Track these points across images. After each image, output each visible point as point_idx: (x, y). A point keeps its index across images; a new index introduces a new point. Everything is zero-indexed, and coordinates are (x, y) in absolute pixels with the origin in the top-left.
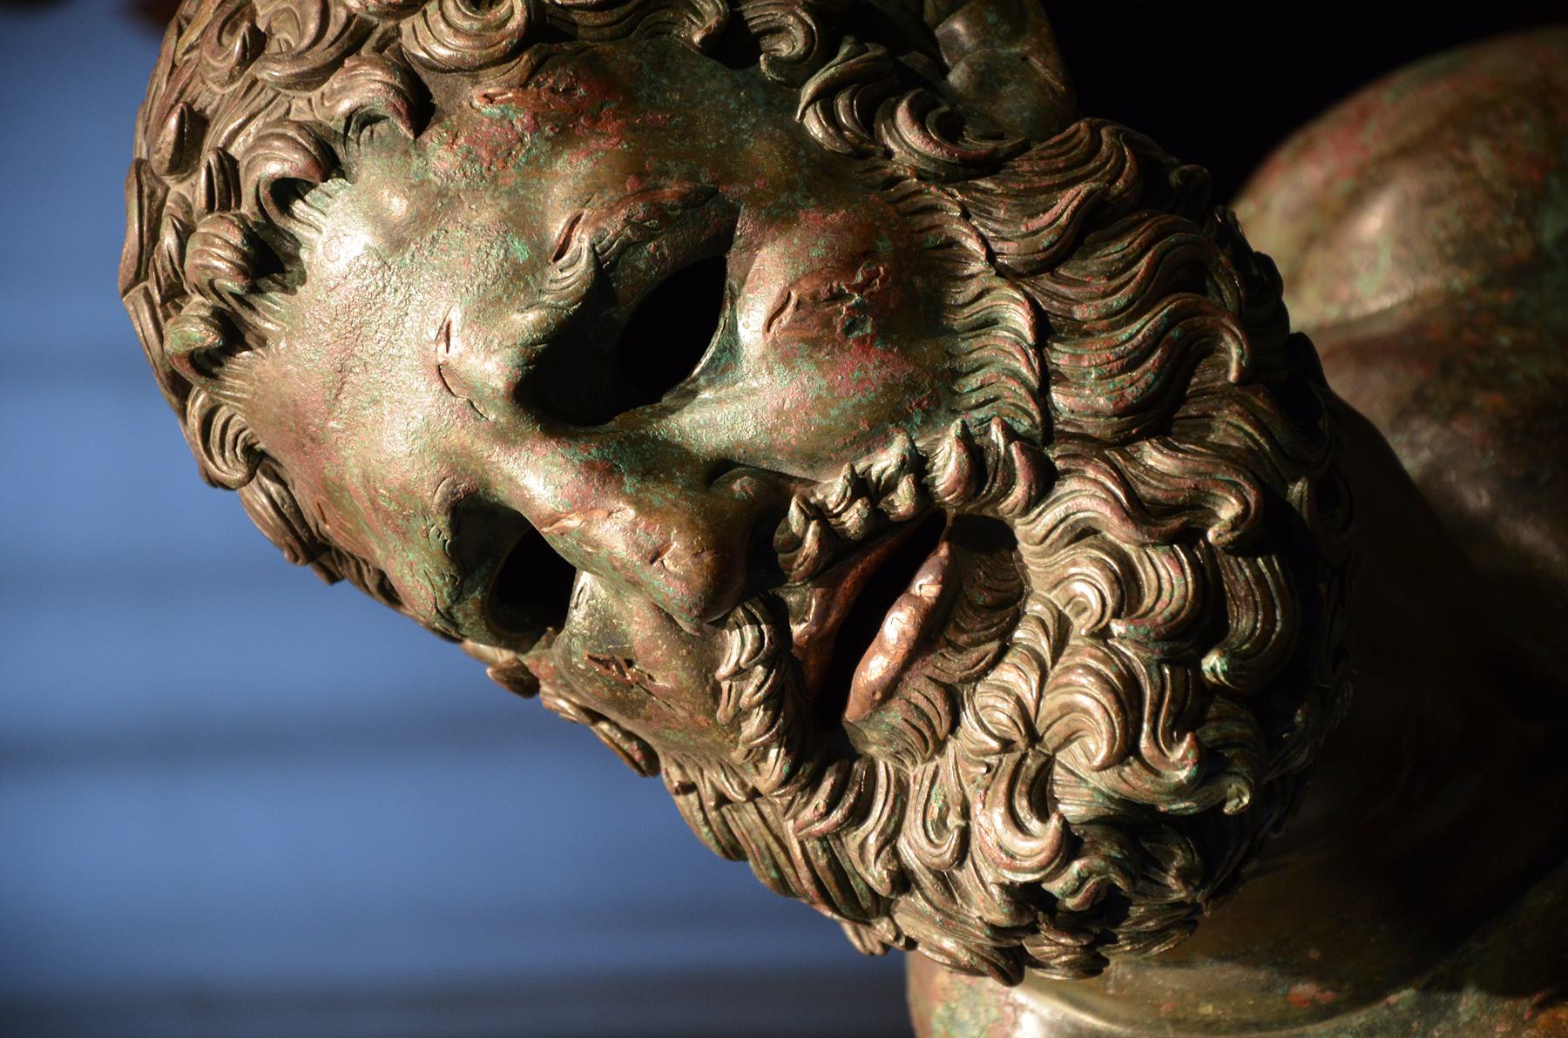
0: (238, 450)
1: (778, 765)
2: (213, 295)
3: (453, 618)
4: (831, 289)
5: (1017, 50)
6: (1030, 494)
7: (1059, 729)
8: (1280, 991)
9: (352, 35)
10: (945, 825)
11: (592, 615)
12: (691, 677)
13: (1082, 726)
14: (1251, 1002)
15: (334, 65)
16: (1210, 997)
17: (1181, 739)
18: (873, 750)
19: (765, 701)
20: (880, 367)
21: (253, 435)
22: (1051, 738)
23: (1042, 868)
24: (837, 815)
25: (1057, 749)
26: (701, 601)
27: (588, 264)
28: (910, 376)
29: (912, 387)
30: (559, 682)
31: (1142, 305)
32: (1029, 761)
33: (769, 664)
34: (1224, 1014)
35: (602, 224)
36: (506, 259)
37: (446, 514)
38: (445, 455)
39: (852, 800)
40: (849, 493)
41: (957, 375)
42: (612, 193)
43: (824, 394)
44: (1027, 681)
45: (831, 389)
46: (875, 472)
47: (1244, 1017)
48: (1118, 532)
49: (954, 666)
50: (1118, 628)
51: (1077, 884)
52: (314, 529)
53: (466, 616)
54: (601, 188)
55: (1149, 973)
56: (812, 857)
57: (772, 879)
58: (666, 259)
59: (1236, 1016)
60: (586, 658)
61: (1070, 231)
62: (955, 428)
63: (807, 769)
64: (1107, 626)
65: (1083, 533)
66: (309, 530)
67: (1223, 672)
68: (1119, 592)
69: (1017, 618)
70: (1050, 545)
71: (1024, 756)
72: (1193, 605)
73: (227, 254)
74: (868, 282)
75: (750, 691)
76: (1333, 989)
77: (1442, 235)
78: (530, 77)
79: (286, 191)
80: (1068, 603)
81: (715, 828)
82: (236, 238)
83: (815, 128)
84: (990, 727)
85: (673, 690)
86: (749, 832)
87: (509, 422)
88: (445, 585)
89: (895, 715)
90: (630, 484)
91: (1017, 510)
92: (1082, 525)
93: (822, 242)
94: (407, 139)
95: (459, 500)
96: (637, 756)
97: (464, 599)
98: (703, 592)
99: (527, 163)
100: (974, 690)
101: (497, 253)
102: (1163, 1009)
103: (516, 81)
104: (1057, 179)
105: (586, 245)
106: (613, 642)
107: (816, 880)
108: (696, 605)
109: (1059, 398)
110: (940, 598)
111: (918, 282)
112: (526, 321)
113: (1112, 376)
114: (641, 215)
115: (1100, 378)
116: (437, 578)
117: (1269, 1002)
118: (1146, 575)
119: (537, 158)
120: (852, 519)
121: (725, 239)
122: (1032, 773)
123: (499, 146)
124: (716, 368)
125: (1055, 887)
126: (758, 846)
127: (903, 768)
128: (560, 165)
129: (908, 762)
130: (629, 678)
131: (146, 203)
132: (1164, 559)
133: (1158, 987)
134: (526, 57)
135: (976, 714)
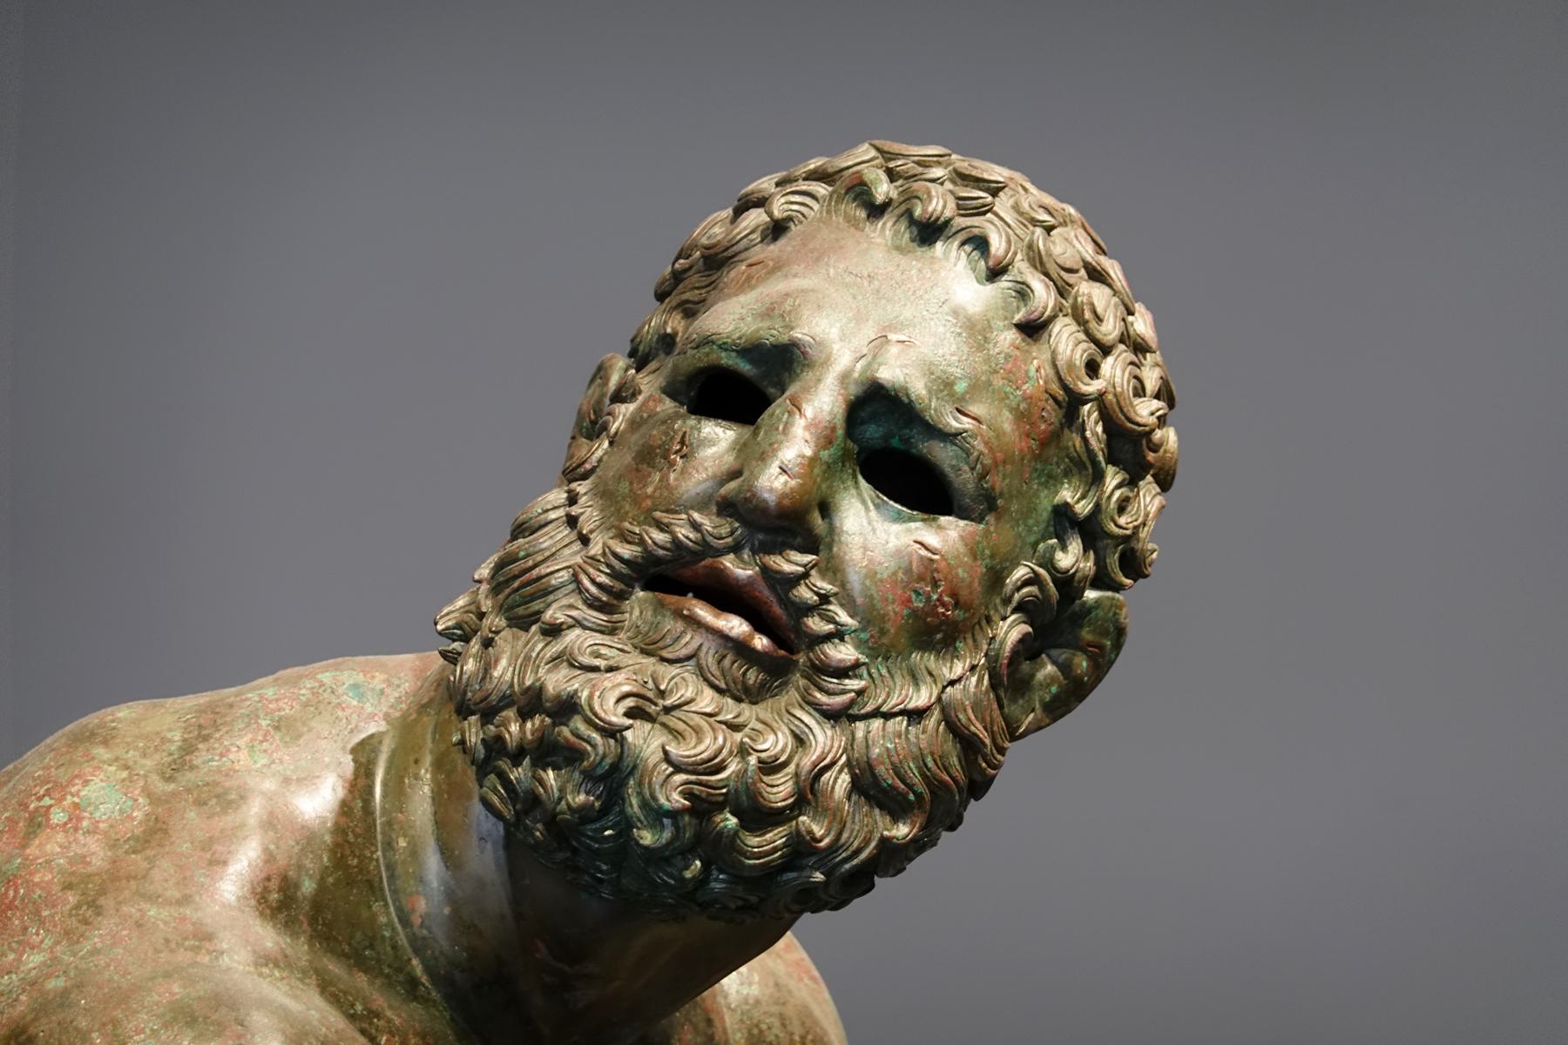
0: (790, 213)
2: (902, 199)
4: (940, 580)
5: (1037, 706)
7: (681, 726)
9: (1064, 287)
10: (596, 657)
13: (688, 741)
15: (1047, 275)
17: (685, 799)
19: (676, 542)
20: (894, 612)
21: (801, 222)
22: (670, 720)
23: (596, 714)
24: (593, 589)
25: (664, 725)
27: (957, 429)
28: (889, 630)
29: (883, 632)
30: (645, 415)
31: (927, 776)
32: (653, 707)
33: (704, 543)
35: (979, 438)
36: (956, 378)
39: (604, 599)
41: (886, 658)
42: (996, 444)
43: (879, 576)
44: (707, 705)
45: (881, 581)
46: (831, 607)
48: (807, 760)
50: (753, 760)
52: (735, 259)
53: (707, 355)
54: (998, 437)
56: (556, 575)
57: (518, 553)
58: (957, 476)
60: (684, 430)
61: (966, 732)
62: (863, 659)
63: (624, 569)
64: (750, 754)
65: (800, 741)
66: (733, 257)
67: (726, 827)
68: (770, 760)
69: (739, 700)
71: (656, 704)
72: (765, 806)
73: (940, 208)
74: (944, 605)
75: (684, 533)
76: (422, 923)
77: (764, 1027)
78: (1050, 395)
79: (980, 243)
80: (753, 729)
81: (542, 516)
82: (948, 214)
83: (1021, 573)
84: (673, 682)
86: (551, 537)
88: (734, 340)
89: (671, 625)
90: (825, 454)
91: (811, 698)
93: (966, 575)
94: (1013, 318)
95: (799, 349)
96: (588, 466)
99: (1005, 393)
101: (958, 372)
103: (1049, 386)
104: (989, 726)
105: (967, 426)
107: (540, 578)
109: (877, 724)
110: (754, 650)
111: (939, 636)
112: (918, 388)
113: (889, 757)
114: (985, 462)
115: (888, 749)
116: (737, 335)
118: (778, 778)
119: (1008, 398)
120: (804, 593)
121: (963, 515)
122: (648, 710)
123: (1014, 374)
125: (578, 724)
128: (1007, 414)
130: (672, 457)
131: (935, 159)
132: (789, 789)
134: (1061, 393)
135: (678, 674)
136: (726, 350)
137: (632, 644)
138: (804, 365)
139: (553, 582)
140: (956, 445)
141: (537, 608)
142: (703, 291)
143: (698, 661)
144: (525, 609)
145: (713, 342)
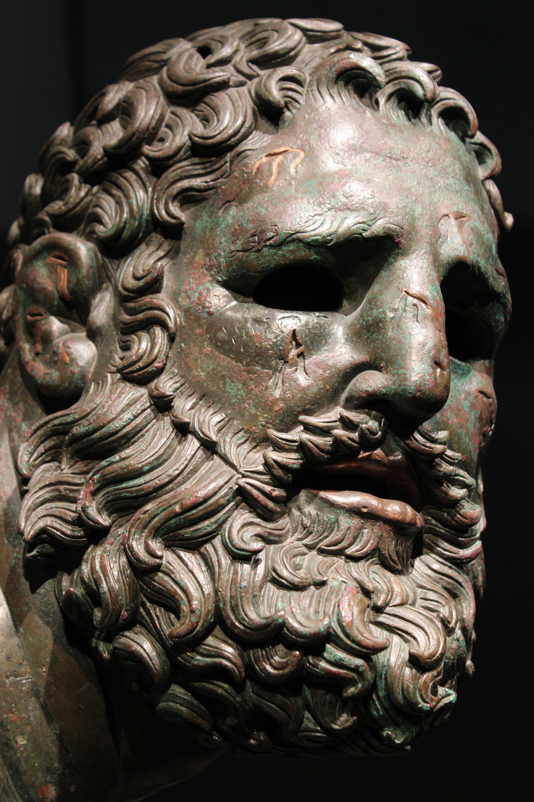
1: (293, 461)
3: (288, 243)
11: (321, 327)
12: (316, 394)
14: (37, 765)
16: (33, 740)
18: (296, 512)
21: (295, 107)
34: (22, 752)
37: (384, 233)
38: (413, 226)
47: (22, 763)
51: (353, 667)
53: (293, 252)
55: (33, 699)
59: (22, 759)
63: (289, 477)
70: (441, 579)
85: (299, 385)
86: (169, 447)
87: (442, 261)
92: (458, 593)
97: (309, 250)
98: (432, 396)
100: (376, 564)
102: (11, 715)
106: (312, 343)
108: (424, 393)
117: (40, 775)
124: (455, 368)
127: (290, 534)
129: (297, 535)
133: (26, 707)
137: (306, 546)
138: (398, 254)
139: (222, 501)
140: (499, 302)
141: (209, 529)
142: (208, 178)
143: (380, 551)
144: (193, 531)
145: (300, 240)
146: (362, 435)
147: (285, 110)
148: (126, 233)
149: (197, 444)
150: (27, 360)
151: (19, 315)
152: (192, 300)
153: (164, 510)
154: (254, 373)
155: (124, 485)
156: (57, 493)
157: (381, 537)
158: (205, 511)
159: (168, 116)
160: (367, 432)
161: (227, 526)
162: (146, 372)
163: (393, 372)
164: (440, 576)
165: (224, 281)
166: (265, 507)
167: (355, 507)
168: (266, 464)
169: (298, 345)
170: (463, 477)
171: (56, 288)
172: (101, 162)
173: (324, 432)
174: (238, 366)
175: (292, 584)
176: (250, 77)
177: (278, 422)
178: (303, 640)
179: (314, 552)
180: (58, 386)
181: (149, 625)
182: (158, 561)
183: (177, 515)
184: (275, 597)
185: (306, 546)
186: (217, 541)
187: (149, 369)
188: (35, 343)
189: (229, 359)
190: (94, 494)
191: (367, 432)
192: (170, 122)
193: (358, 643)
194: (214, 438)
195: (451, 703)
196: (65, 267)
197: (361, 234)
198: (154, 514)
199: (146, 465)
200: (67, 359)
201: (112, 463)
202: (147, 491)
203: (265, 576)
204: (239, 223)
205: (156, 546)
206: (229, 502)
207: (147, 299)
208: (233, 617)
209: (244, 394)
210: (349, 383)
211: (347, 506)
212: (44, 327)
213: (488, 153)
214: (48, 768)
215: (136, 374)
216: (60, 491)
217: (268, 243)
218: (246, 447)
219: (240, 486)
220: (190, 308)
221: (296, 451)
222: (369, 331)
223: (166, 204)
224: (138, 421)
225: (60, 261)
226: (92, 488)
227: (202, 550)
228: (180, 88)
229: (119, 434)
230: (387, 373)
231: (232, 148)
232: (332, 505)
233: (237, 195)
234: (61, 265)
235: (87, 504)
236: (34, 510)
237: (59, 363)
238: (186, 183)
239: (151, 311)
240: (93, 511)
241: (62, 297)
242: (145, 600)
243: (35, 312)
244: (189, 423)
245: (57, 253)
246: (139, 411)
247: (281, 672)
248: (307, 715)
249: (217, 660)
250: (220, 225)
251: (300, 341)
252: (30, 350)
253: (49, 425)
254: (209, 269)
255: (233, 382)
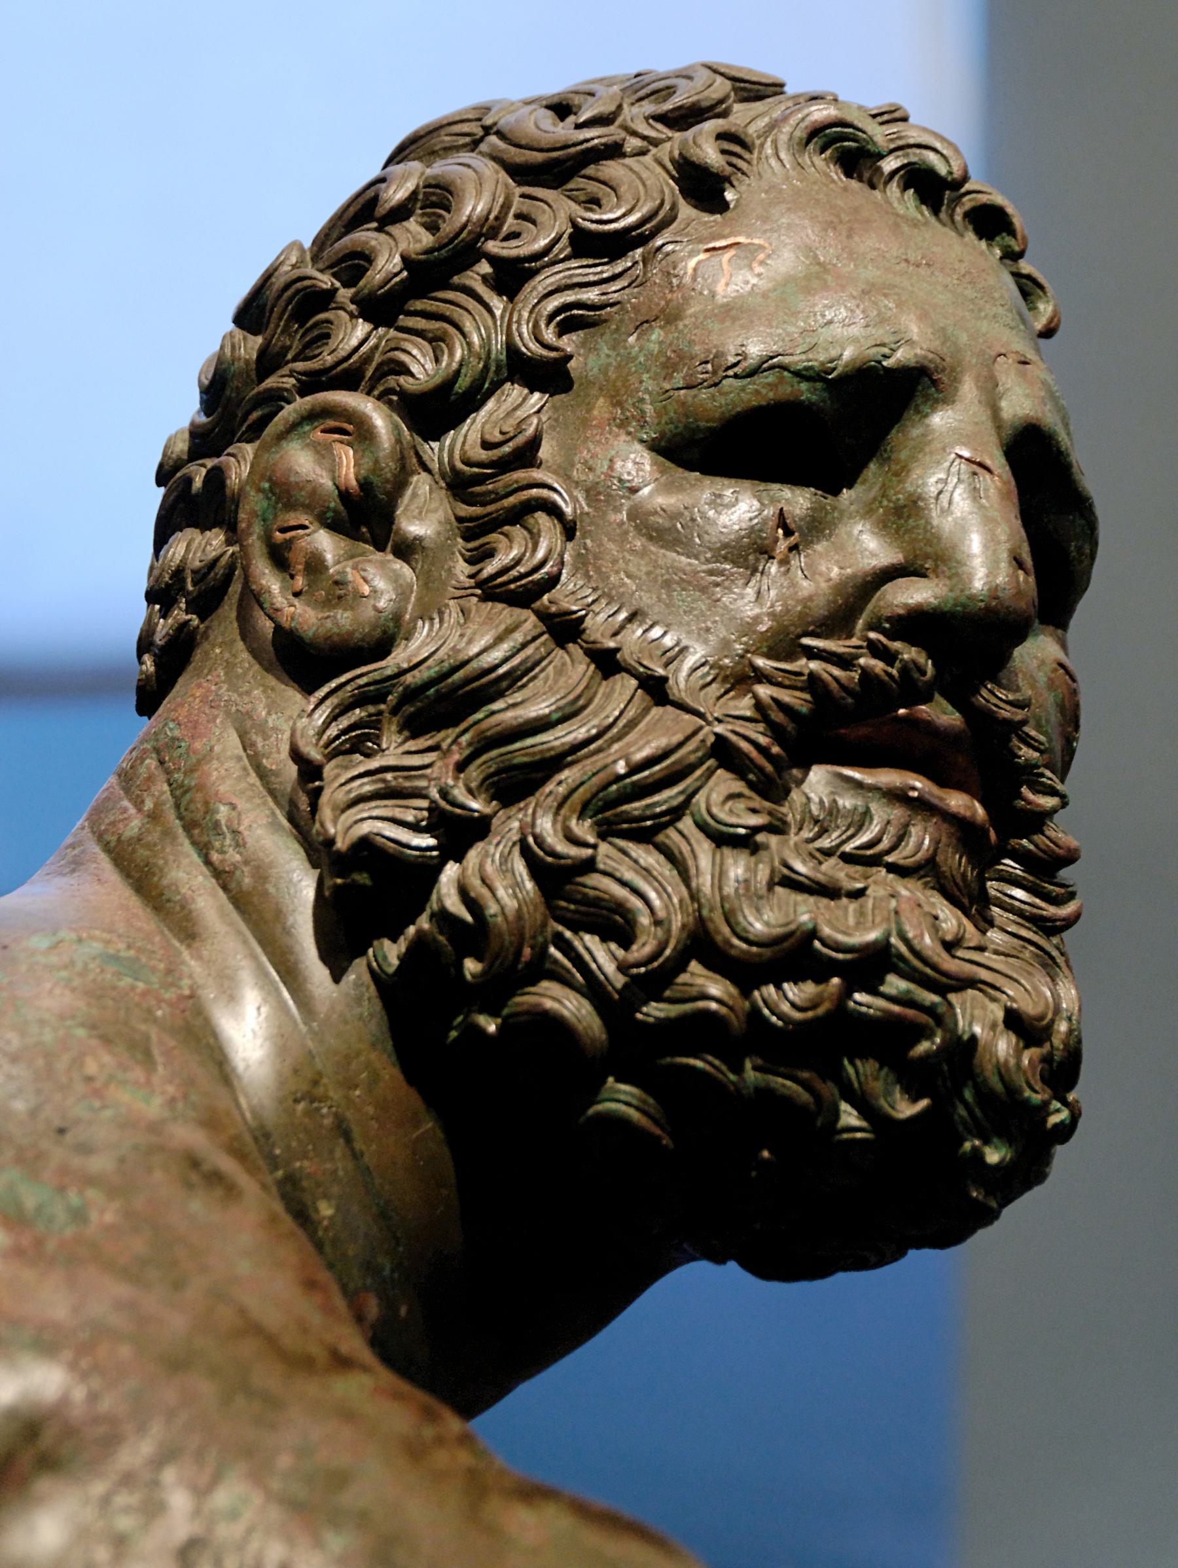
3: (765, 370)
6: (1059, 920)
8: (369, 1281)
26: (1007, 608)
34: (326, 1229)
37: (917, 362)
40: (1042, 747)
49: (955, 862)
89: (882, 815)
100: (933, 888)
102: (306, 1163)
117: (355, 1272)
126: (579, 697)
129: (807, 834)
136: (808, 379)
138: (937, 401)
144: (648, 806)
145: (783, 367)
146: (905, 670)
147: (727, 185)
148: (463, 384)
149: (634, 683)
150: (278, 605)
151: (255, 537)
152: (598, 472)
153: (594, 774)
154: (721, 573)
155: (518, 745)
156: (380, 785)
157: (936, 842)
158: (665, 772)
159: (517, 204)
160: (912, 666)
161: (700, 798)
162: (532, 582)
163: (947, 574)
164: (1021, 943)
165: (653, 439)
166: (761, 769)
167: (897, 788)
168: (759, 705)
169: (788, 533)
170: (1051, 779)
171: (333, 479)
172: (397, 279)
173: (845, 662)
174: (690, 564)
175: (818, 883)
176: (655, 143)
177: (765, 650)
178: (849, 956)
179: (833, 861)
180: (351, 634)
181: (568, 971)
182: (590, 851)
183: (619, 778)
184: (792, 903)
185: (819, 850)
186: (686, 824)
187: (536, 576)
188: (292, 577)
189: (674, 555)
190: (461, 767)
191: (912, 666)
192: (525, 209)
193: (934, 967)
194: (661, 671)
195: (1062, 1122)
196: (349, 444)
197: (879, 362)
198: (578, 782)
199: (556, 711)
200: (366, 590)
201: (493, 713)
202: (561, 749)
203: (773, 871)
204: (674, 348)
205: (584, 829)
206: (701, 762)
207: (521, 475)
208: (726, 930)
209: (703, 607)
210: (869, 601)
211: (883, 786)
212: (310, 548)
213: (1041, 293)
214: (369, 1263)
215: (512, 586)
216: (384, 781)
217: (730, 373)
218: (715, 689)
219: (716, 734)
220: (597, 483)
221: (801, 689)
222: (900, 517)
223: (536, 325)
224: (529, 651)
225: (337, 436)
226: (457, 757)
227: (660, 838)
228: (539, 157)
229: (501, 671)
230: (937, 577)
231: (643, 240)
232: (859, 785)
233: (663, 311)
234: (342, 442)
235: (450, 782)
236: (343, 811)
237: (350, 598)
238: (570, 297)
239: (525, 492)
240: (460, 794)
241: (344, 495)
242: (560, 928)
243: (292, 523)
244: (617, 650)
245: (331, 423)
246: (529, 638)
247: (810, 1014)
248: (844, 1106)
249: (701, 1004)
250: (636, 358)
251: (793, 526)
252: (283, 589)
253: (349, 688)
254: (623, 424)
255: (683, 589)
